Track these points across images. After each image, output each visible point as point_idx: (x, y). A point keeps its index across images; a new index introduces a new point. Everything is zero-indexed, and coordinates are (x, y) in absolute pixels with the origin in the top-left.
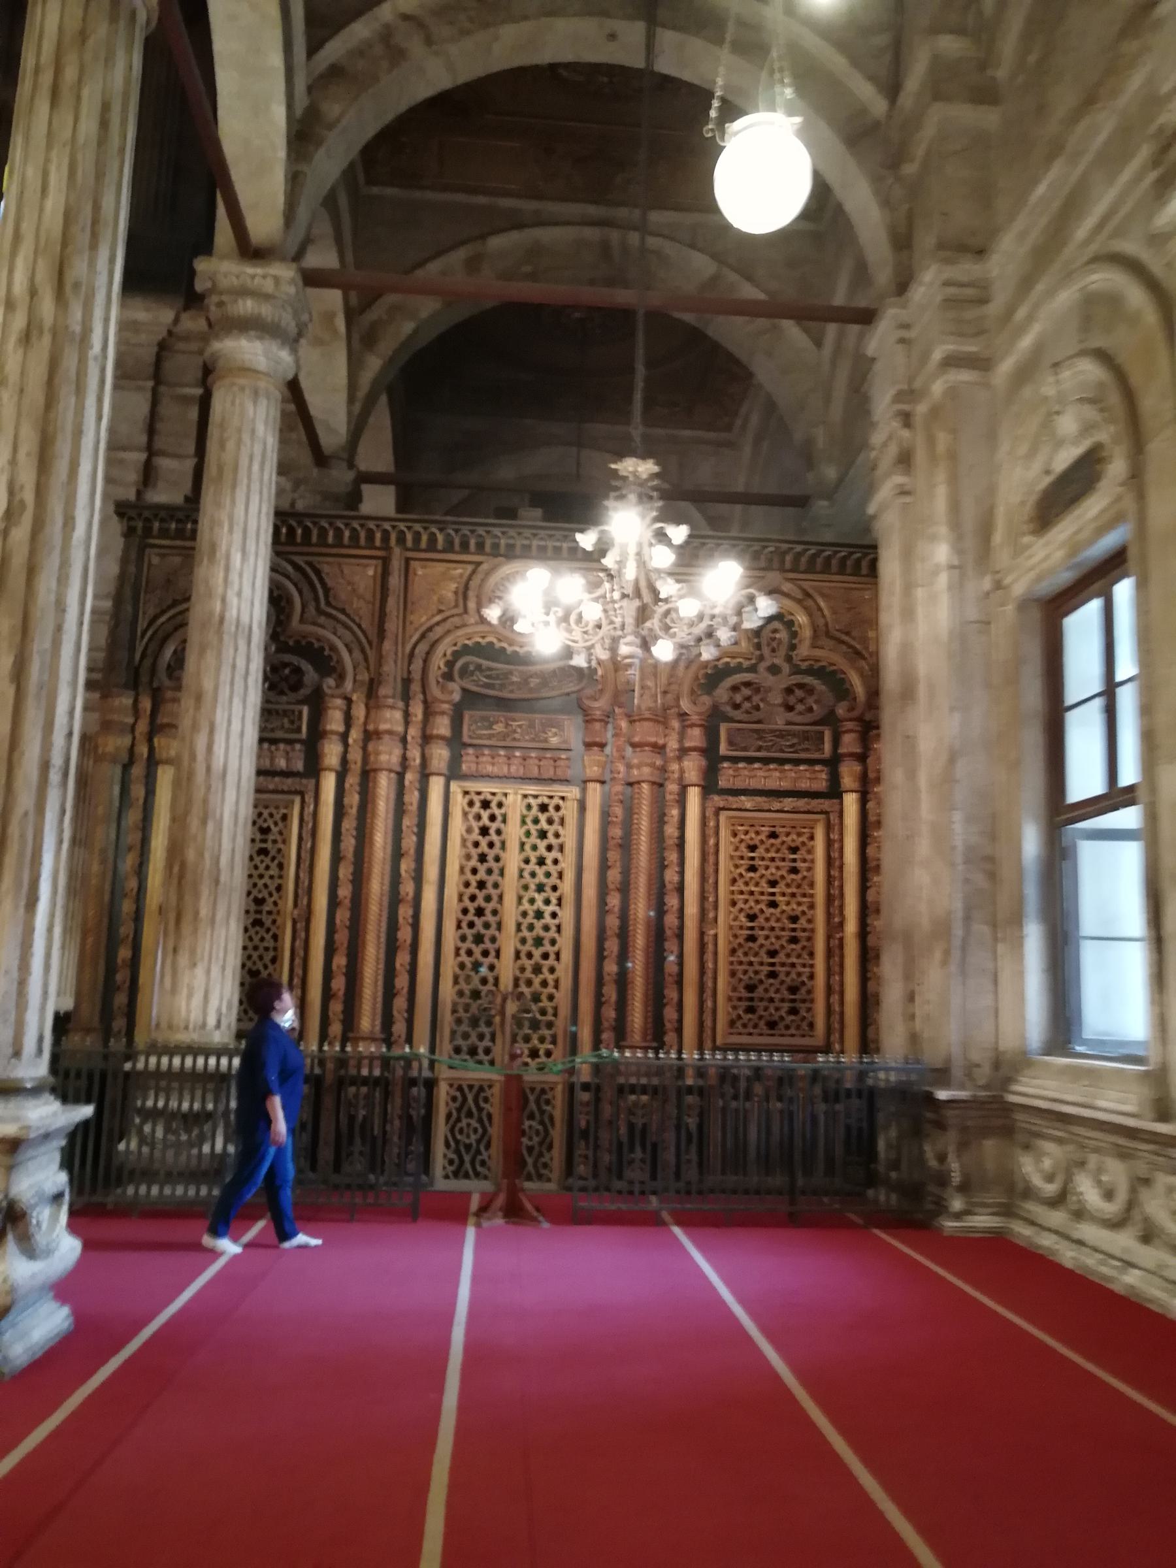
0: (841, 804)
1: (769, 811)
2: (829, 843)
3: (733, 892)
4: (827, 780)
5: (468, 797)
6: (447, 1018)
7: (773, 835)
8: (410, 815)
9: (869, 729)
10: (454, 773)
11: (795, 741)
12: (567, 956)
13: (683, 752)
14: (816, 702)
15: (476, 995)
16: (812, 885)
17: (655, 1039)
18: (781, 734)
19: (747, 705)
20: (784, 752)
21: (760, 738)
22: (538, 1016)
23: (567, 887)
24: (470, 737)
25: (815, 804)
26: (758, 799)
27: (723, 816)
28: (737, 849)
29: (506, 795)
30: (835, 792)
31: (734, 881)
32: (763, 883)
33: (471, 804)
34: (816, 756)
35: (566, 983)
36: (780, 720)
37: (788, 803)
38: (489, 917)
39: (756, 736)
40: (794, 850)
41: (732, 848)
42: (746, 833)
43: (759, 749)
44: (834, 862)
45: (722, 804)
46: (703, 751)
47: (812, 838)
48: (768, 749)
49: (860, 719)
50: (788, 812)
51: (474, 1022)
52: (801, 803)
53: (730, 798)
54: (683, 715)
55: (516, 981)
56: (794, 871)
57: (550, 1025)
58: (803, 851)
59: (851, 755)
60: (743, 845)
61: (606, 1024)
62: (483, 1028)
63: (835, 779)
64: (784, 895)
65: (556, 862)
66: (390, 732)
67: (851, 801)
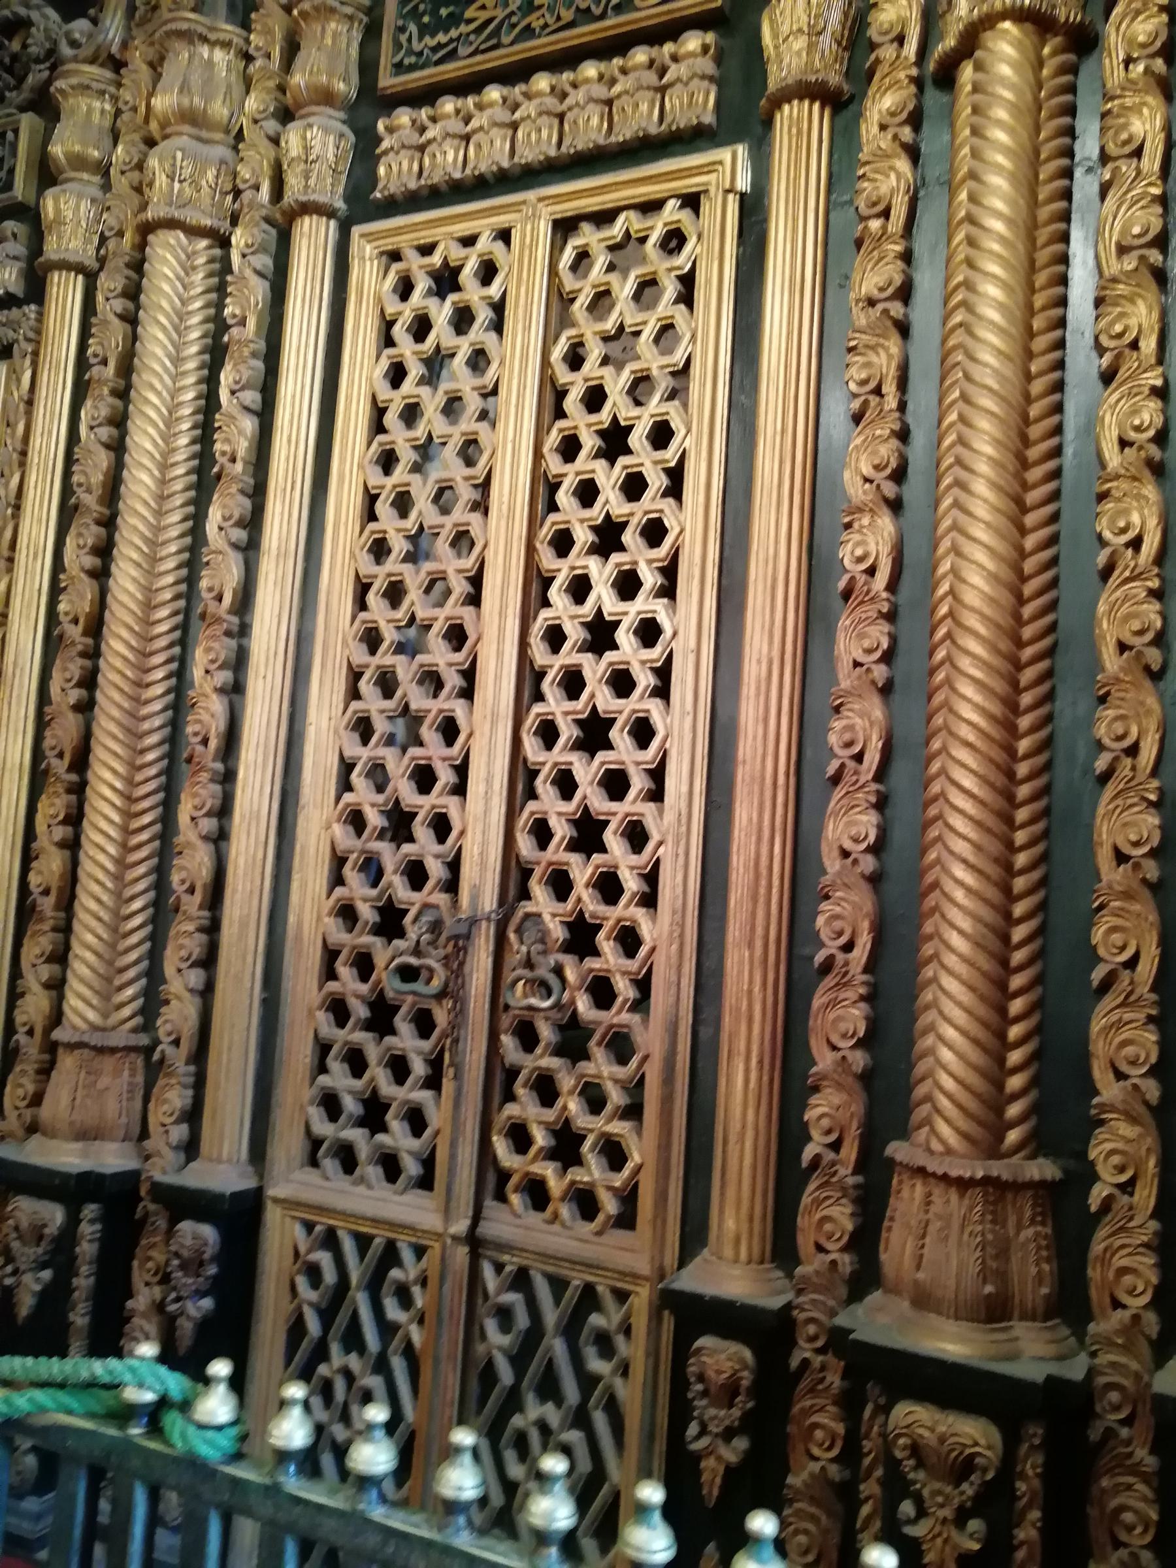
5: (396, 267)
6: (303, 986)
8: (239, 353)
10: (363, 203)
12: (685, 781)
15: (391, 922)
17: (1037, 1145)
22: (583, 1005)
23: (694, 524)
24: (399, 68)
29: (504, 236)
33: (405, 289)
35: (680, 883)
38: (440, 655)
51: (381, 1018)
55: (516, 878)
57: (621, 1046)
61: (824, 1060)
62: (406, 1039)
65: (661, 435)
66: (192, 118)
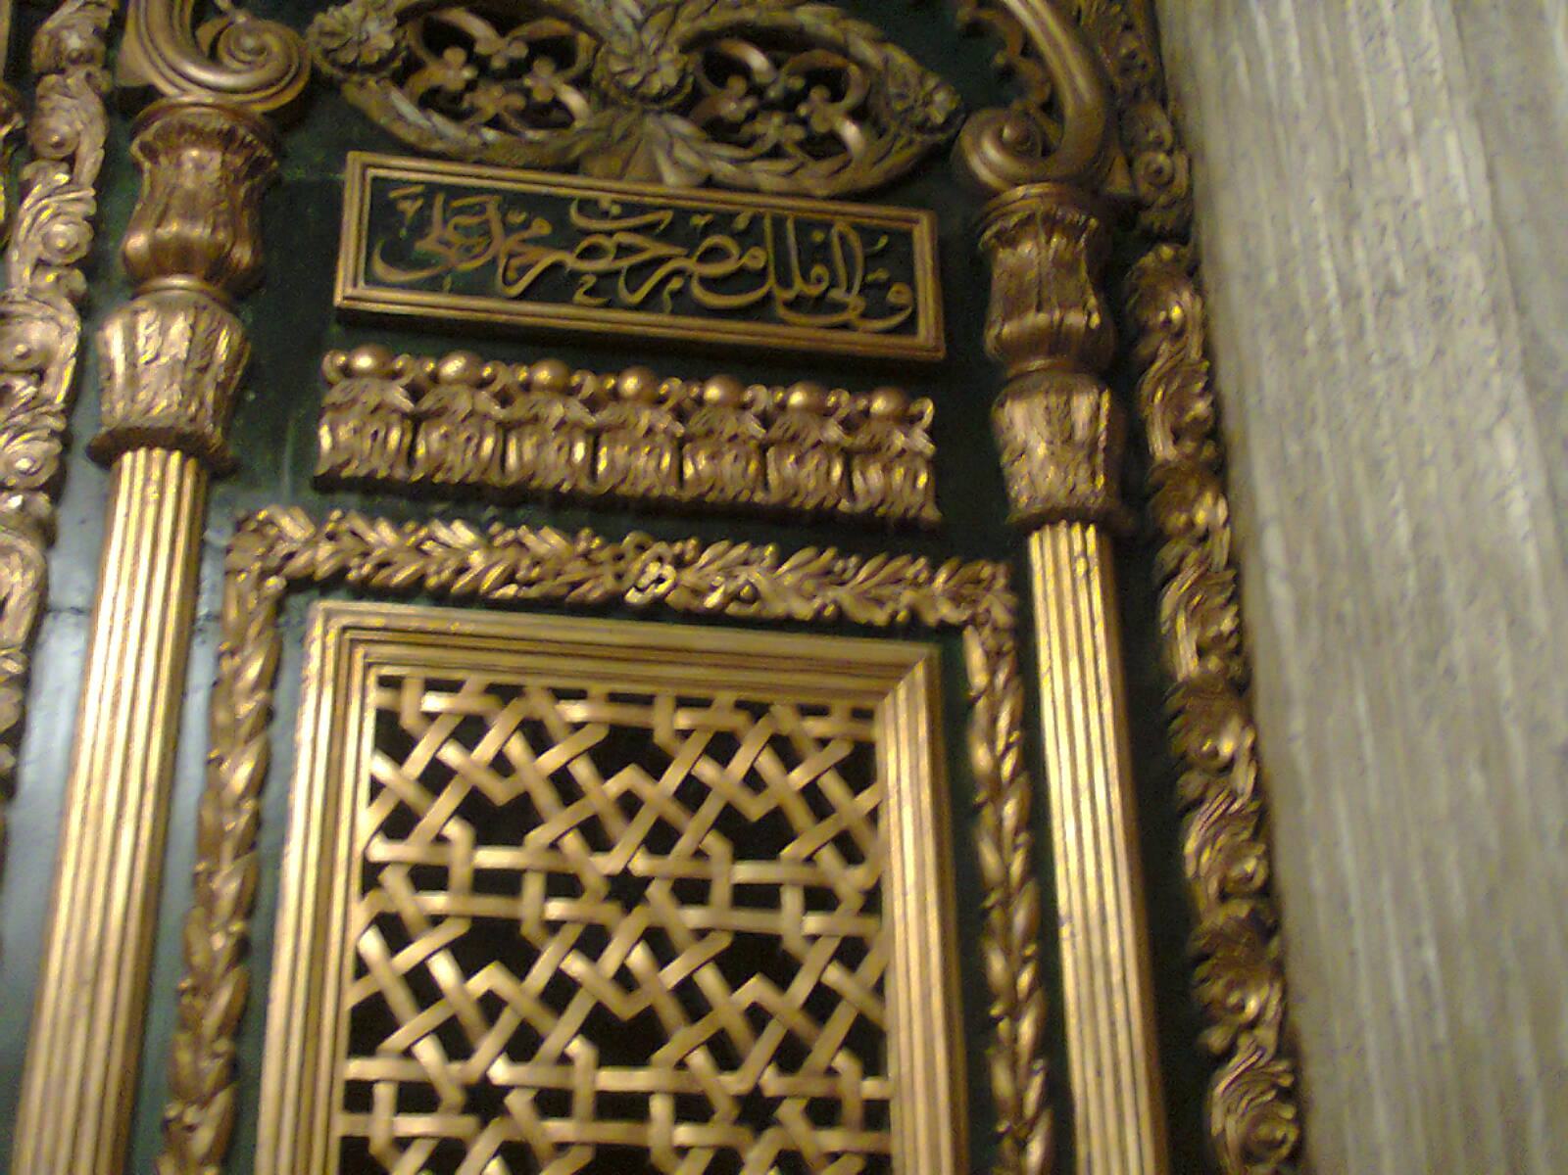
0: (1021, 585)
1: (612, 607)
2: (958, 803)
3: (359, 1096)
4: (935, 465)
7: (626, 747)
9: (1141, 232)
11: (757, 258)
13: (101, 281)
14: (858, 115)
16: (868, 1044)
18: (679, 229)
19: (491, 99)
20: (683, 304)
21: (565, 236)
25: (863, 585)
26: (549, 541)
27: (323, 628)
28: (399, 824)
30: (976, 521)
31: (370, 1026)
32: (564, 1035)
34: (867, 337)
36: (676, 163)
37: (721, 572)
39: (542, 227)
40: (758, 837)
41: (370, 818)
42: (469, 731)
43: (553, 285)
44: (991, 906)
45: (324, 557)
46: (231, 290)
47: (860, 769)
48: (603, 289)
49: (1085, 185)
50: (716, 619)
52: (785, 581)
53: (383, 534)
54: (129, 106)
56: (755, 956)
58: (810, 837)
59: (1054, 341)
60: (440, 811)
63: (969, 457)
64: (691, 1107)
67: (1067, 576)
